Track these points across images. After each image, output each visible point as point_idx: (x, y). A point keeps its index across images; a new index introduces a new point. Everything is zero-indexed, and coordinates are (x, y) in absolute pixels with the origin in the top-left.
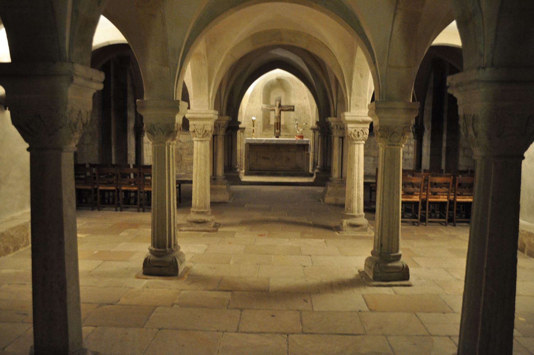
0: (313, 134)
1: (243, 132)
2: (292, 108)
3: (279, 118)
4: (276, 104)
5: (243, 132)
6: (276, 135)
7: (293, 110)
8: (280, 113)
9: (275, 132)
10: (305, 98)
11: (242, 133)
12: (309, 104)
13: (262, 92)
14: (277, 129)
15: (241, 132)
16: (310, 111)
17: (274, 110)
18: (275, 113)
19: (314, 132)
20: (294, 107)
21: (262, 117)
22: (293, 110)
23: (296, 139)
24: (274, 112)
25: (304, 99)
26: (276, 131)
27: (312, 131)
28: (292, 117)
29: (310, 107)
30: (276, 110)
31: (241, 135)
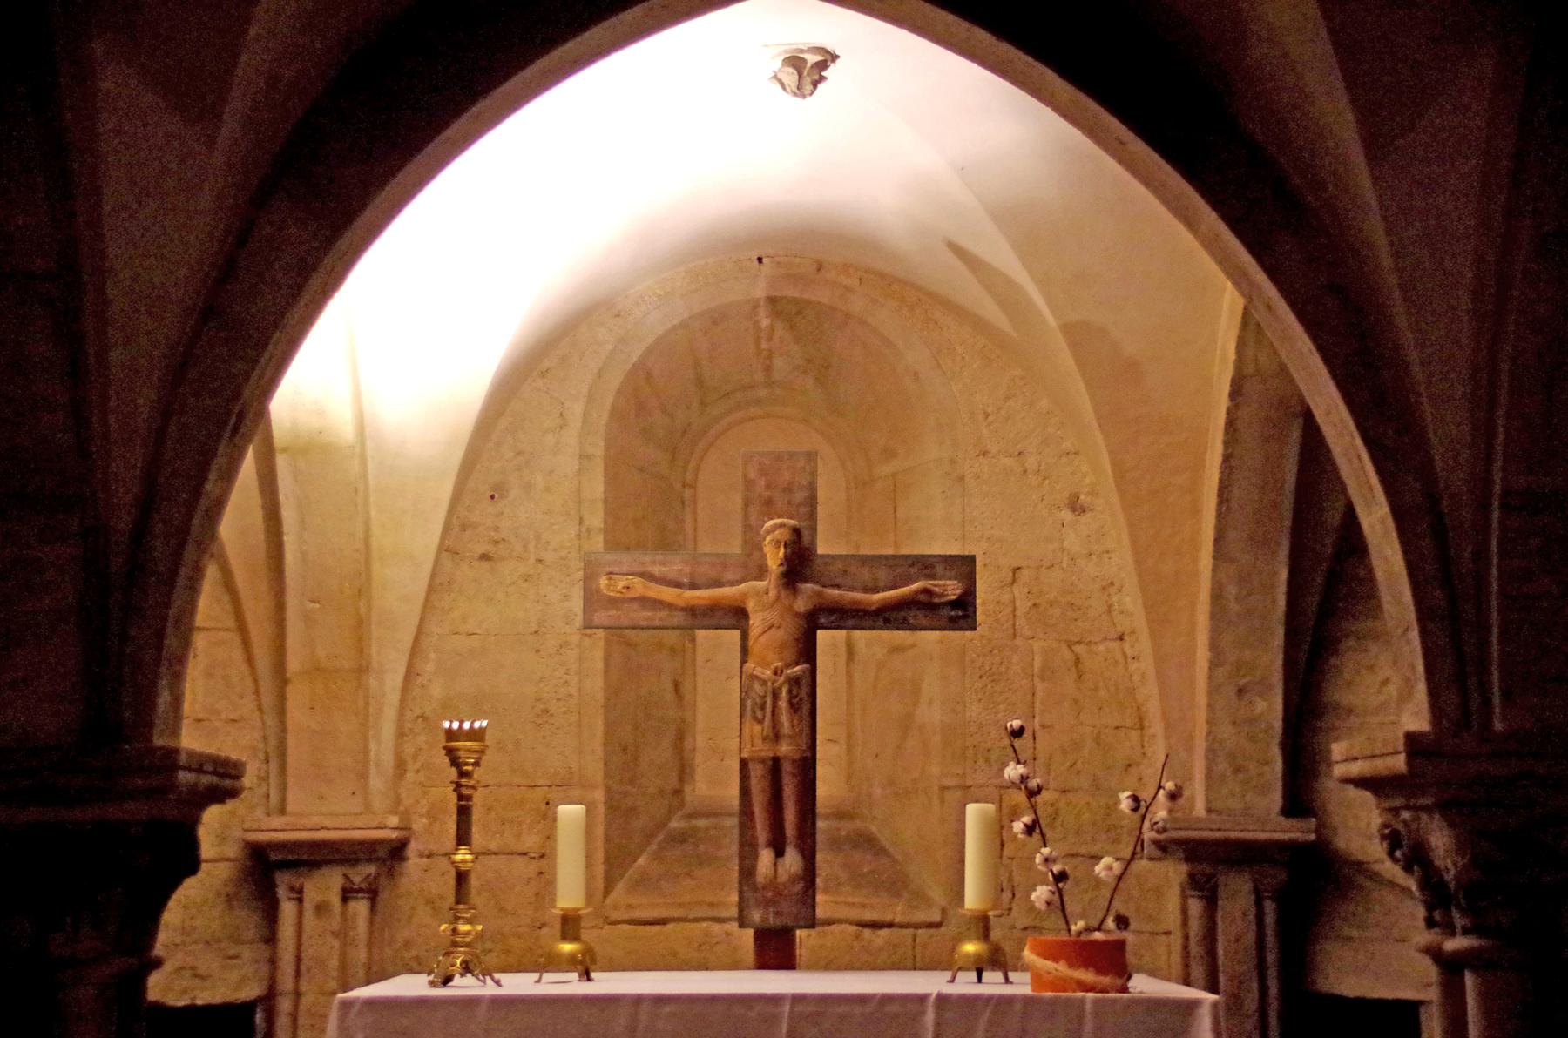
0: (1196, 906)
1: (373, 894)
2: (951, 589)
3: (794, 707)
4: (753, 544)
5: (373, 894)
6: (756, 916)
7: (961, 612)
8: (807, 652)
9: (747, 873)
10: (1076, 507)
11: (360, 907)
12: (1121, 563)
13: (599, 451)
14: (779, 853)
15: (347, 894)
16: (1143, 644)
17: (738, 615)
18: (745, 651)
19: (1204, 887)
20: (965, 566)
21: (598, 726)
22: (961, 612)
23: (1038, 980)
24: (736, 635)
25: (1067, 515)
26: (766, 857)
27: (1174, 872)
28: (932, 714)
29: (1130, 600)
30: (756, 621)
31: (343, 934)
